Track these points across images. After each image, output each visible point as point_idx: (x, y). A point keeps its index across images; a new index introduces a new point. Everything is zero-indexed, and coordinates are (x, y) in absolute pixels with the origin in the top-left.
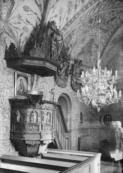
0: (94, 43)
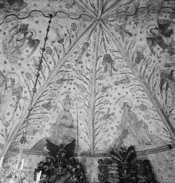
0: (134, 106)
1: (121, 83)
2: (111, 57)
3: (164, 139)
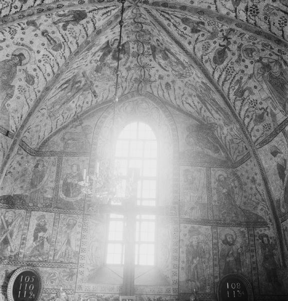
0: (24, 67)
1: (48, 39)
2: (83, 19)
3: (11, 122)
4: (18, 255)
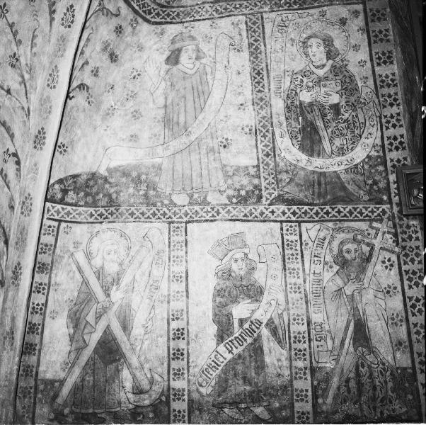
4: (168, 403)
